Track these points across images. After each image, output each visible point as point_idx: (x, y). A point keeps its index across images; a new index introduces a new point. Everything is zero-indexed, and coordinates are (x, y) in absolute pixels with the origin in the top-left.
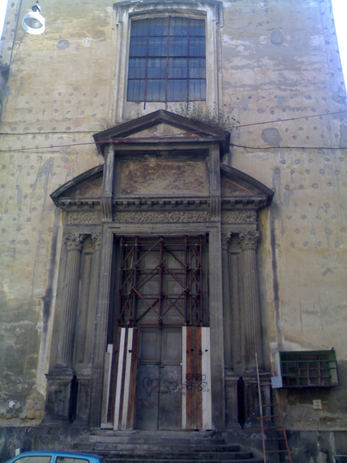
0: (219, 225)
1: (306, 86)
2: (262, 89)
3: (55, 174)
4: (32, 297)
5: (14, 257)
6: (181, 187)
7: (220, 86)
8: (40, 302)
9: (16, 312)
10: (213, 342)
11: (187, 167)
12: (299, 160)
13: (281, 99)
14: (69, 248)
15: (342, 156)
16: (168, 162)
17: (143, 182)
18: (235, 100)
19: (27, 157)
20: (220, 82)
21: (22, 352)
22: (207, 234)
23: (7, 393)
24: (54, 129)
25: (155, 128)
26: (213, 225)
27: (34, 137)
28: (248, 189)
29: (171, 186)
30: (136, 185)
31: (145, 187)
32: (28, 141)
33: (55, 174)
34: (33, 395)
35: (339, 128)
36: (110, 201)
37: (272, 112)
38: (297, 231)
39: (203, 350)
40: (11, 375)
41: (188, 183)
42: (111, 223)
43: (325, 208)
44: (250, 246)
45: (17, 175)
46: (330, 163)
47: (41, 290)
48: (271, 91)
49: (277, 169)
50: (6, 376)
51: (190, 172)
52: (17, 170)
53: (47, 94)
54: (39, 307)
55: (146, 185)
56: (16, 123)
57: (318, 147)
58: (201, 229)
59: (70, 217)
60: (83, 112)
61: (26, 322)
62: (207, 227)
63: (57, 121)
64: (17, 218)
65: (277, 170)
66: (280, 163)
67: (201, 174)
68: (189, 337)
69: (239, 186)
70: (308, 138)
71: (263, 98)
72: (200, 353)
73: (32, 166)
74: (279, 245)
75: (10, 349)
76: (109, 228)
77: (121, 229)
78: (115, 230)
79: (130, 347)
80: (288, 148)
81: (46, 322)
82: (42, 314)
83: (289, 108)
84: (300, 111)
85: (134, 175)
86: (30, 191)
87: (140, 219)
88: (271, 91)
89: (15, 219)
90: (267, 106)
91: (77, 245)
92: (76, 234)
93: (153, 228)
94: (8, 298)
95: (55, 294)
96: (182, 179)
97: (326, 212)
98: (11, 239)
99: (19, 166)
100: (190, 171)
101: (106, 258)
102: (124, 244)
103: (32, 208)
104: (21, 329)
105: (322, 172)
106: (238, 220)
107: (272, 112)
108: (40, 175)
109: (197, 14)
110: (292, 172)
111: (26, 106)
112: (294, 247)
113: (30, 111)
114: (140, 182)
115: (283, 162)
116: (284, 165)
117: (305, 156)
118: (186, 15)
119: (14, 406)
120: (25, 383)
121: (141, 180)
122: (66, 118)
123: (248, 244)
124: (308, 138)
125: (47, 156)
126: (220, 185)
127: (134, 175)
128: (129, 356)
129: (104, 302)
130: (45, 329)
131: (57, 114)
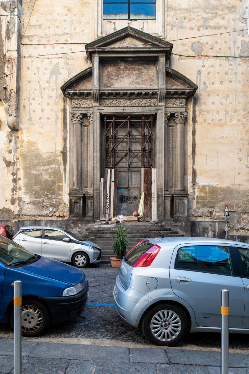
0: (163, 108)
1: (222, 10)
2: (194, 12)
3: (61, 73)
4: (55, 151)
6: (140, 82)
7: (166, 9)
8: (60, 154)
9: (48, 160)
10: (158, 177)
11: (144, 69)
12: (213, 65)
13: (206, 20)
14: (74, 122)
15: (240, 62)
16: (132, 65)
17: (117, 80)
18: (175, 20)
19: (42, 61)
20: (166, 5)
21: (54, 182)
22: (156, 114)
23: (48, 204)
24: (57, 41)
26: (160, 108)
27: (45, 47)
28: (182, 84)
29: (134, 82)
30: (112, 81)
31: (118, 83)
32: (40, 50)
33: (61, 73)
35: (240, 43)
36: (98, 92)
37: (199, 30)
38: (208, 112)
39: (153, 181)
40: (49, 195)
41: (145, 80)
43: (226, 97)
44: (181, 121)
46: (232, 67)
47: (60, 148)
48: (199, 14)
49: (199, 71)
50: (47, 195)
51: (146, 73)
53: (50, 14)
54: (60, 157)
55: (118, 81)
56: (32, 36)
57: (225, 56)
58: (153, 110)
59: (74, 103)
60: (75, 29)
61: (54, 166)
62: (156, 109)
63: (59, 35)
64: (41, 103)
65: (199, 72)
66: (201, 67)
67: (153, 74)
68: (145, 173)
69: (177, 82)
70: (220, 49)
71: (194, 19)
72: (151, 183)
73: (46, 68)
74: (197, 121)
75: (47, 180)
76: (98, 109)
77: (105, 110)
78: (102, 111)
79: (113, 179)
80: (207, 56)
82: (62, 161)
83: (210, 27)
84: (216, 29)
85: (111, 75)
86: (46, 85)
87: (116, 104)
88: (199, 14)
89: (39, 104)
90: (196, 25)
91: (79, 121)
92: (78, 113)
95: (68, 150)
96: (141, 77)
97: (226, 100)
98: (39, 117)
100: (146, 72)
101: (97, 128)
102: (106, 120)
103: (49, 96)
104: (51, 170)
105: (227, 73)
106: (174, 105)
107: (199, 30)
108: (52, 73)
110: (209, 73)
111: (37, 23)
112: (205, 122)
113: (40, 26)
114: (115, 80)
115: (203, 66)
116: (204, 68)
117: (217, 61)
119: (52, 210)
120: (57, 199)
121: (115, 78)
122: (65, 33)
123: (179, 120)
124: (220, 49)
125: (55, 61)
126: (165, 81)
127: (111, 75)
128: (113, 184)
129: (97, 154)
130: (65, 170)
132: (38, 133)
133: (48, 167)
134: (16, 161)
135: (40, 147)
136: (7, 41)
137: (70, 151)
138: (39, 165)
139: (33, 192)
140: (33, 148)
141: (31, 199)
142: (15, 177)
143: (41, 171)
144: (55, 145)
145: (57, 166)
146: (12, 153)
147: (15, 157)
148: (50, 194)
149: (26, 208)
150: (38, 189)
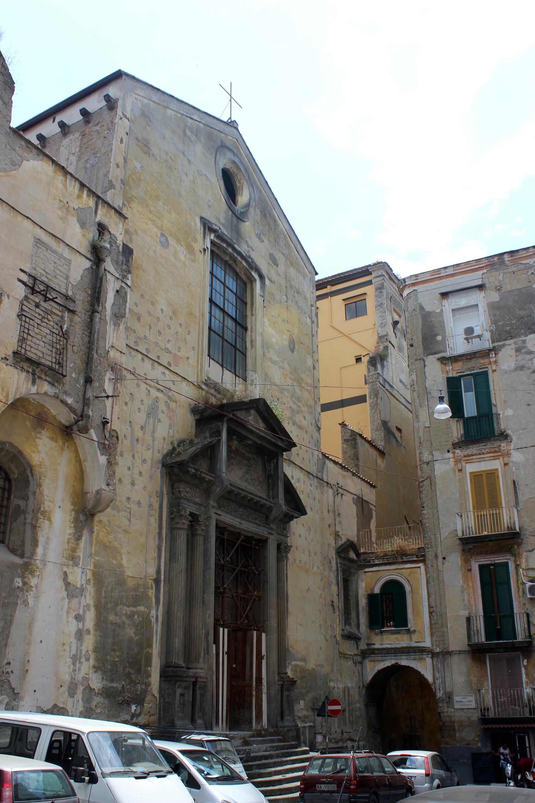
5: (129, 520)
19: (138, 385)
25: (250, 413)
34: (148, 698)
40: (132, 674)
42: (217, 509)
45: (129, 405)
47: (152, 571)
52: (130, 400)
61: (142, 608)
75: (130, 640)
77: (222, 517)
78: (219, 517)
81: (157, 610)
82: (154, 600)
93: (241, 524)
94: (127, 574)
99: (131, 394)
103: (143, 458)
108: (149, 414)
109: (245, 274)
118: (238, 270)
119: (135, 710)
131: (160, 338)
132: (124, 530)
133: (134, 609)
134: (86, 587)
135: (124, 562)
136: (112, 327)
137: (164, 580)
138: (120, 604)
139: (109, 667)
140: (114, 562)
141: (105, 682)
142: (81, 626)
143: (124, 618)
144: (146, 562)
145: (147, 609)
146: (80, 566)
147: (84, 577)
148: (133, 672)
149: (94, 707)
150: (117, 659)
